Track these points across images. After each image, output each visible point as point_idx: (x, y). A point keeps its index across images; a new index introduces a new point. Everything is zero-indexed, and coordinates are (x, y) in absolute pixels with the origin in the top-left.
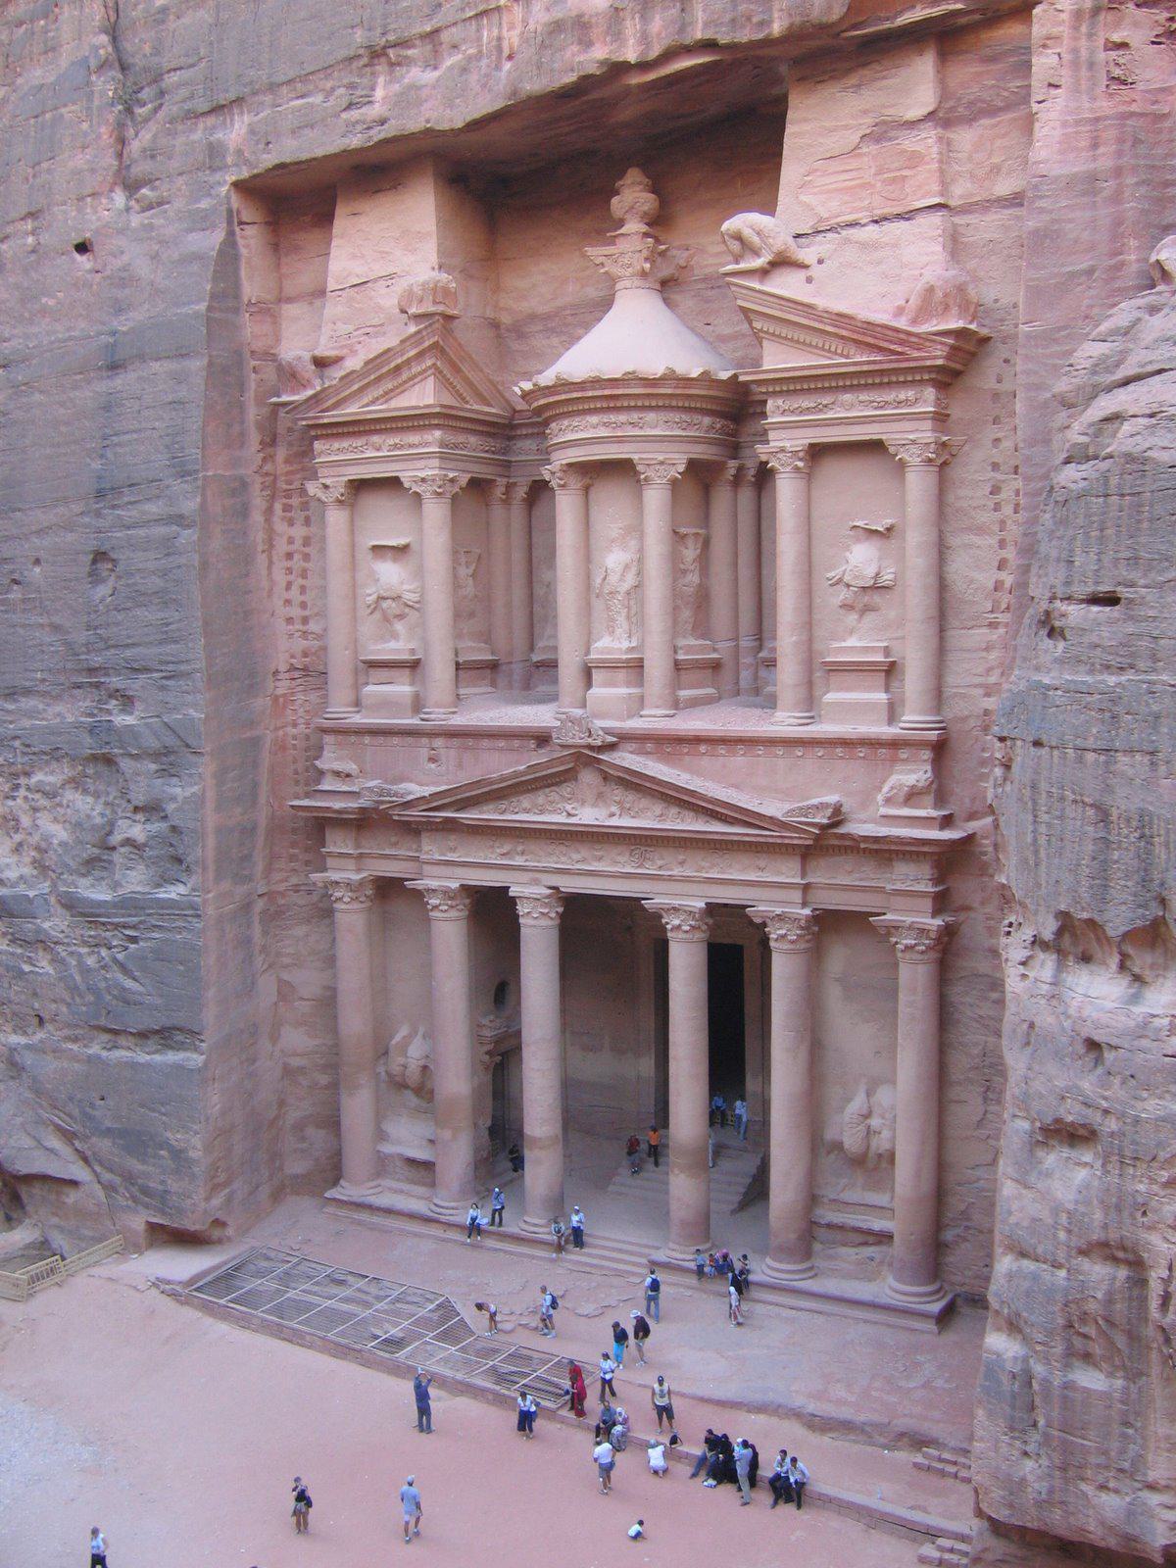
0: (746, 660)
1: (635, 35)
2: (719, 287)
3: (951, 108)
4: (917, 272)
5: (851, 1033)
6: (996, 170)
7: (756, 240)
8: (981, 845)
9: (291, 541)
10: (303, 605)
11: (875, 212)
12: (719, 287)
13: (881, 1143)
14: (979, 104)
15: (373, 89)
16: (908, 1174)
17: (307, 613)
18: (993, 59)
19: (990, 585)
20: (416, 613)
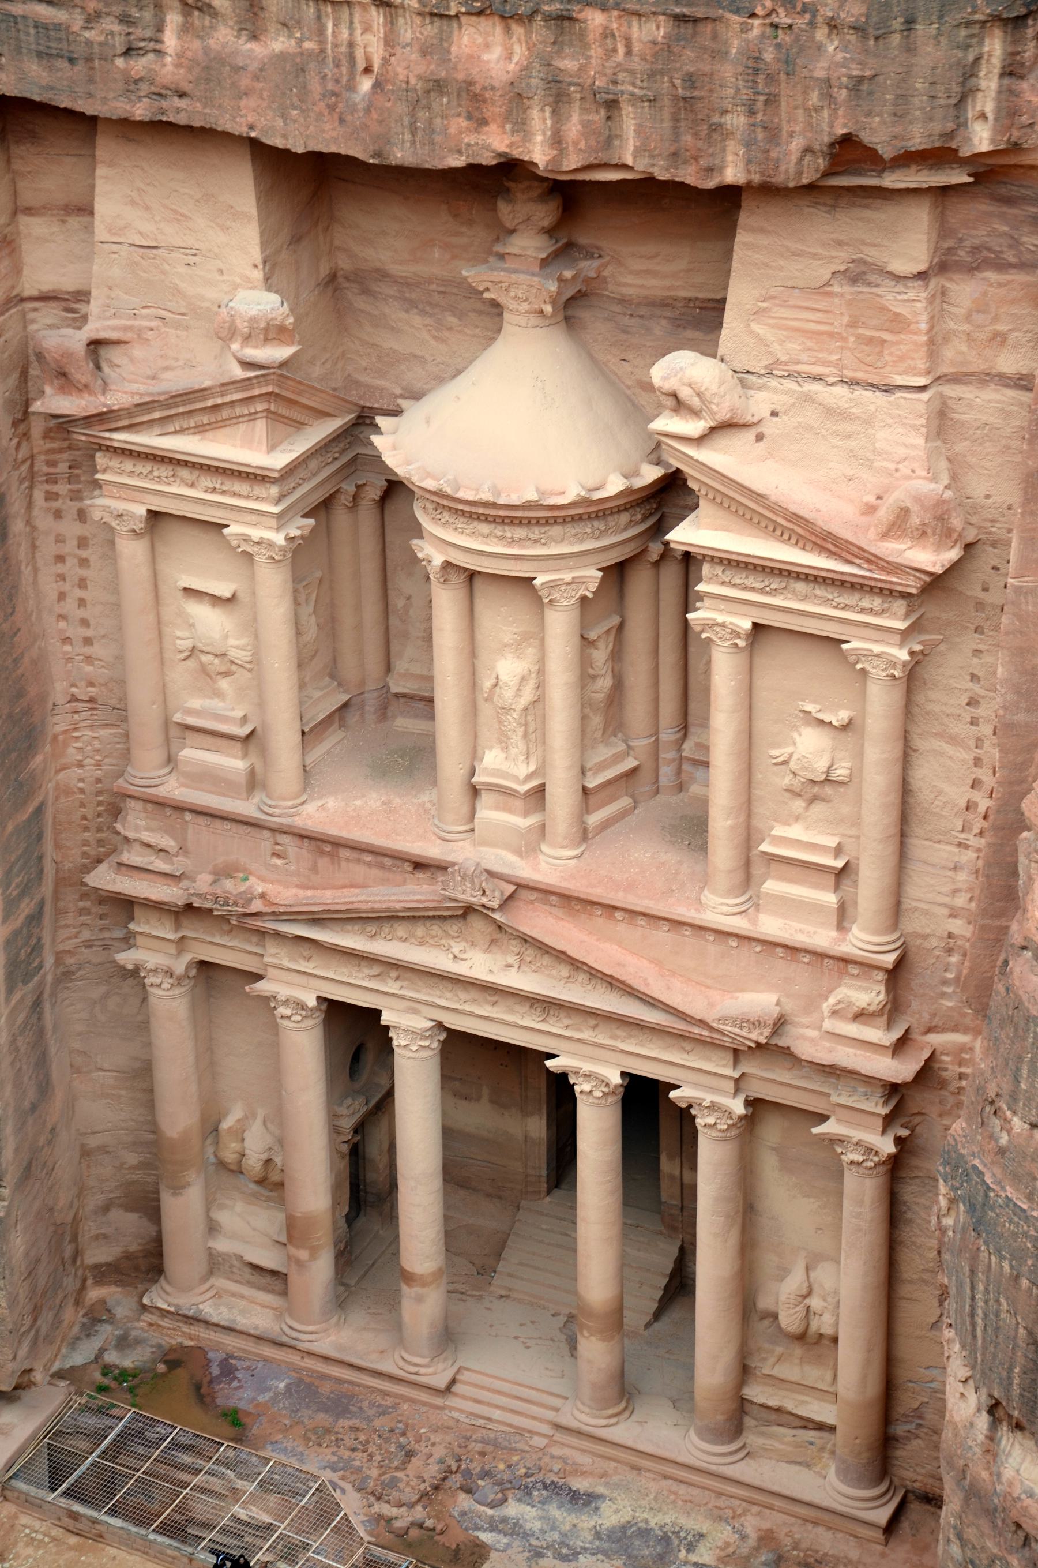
0: (667, 755)
1: (544, 134)
2: (641, 317)
3: (949, 249)
4: (892, 466)
5: (790, 1207)
6: (999, 339)
7: (696, 402)
8: (941, 1062)
9: (60, 539)
10: (85, 623)
11: (845, 372)
12: (641, 317)
13: (824, 1324)
14: (985, 253)
15: (160, 29)
16: (853, 1368)
17: (89, 633)
18: (1009, 201)
19: (964, 804)
20: (248, 675)
